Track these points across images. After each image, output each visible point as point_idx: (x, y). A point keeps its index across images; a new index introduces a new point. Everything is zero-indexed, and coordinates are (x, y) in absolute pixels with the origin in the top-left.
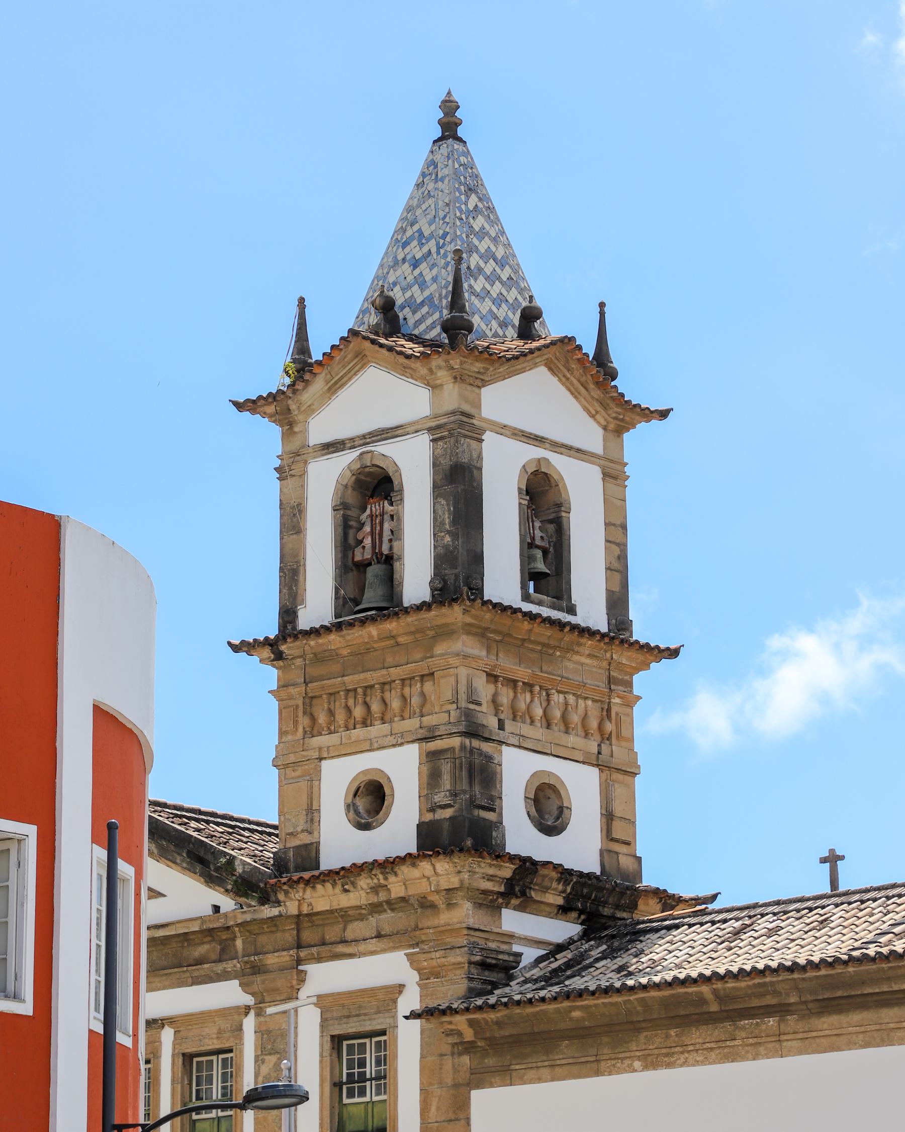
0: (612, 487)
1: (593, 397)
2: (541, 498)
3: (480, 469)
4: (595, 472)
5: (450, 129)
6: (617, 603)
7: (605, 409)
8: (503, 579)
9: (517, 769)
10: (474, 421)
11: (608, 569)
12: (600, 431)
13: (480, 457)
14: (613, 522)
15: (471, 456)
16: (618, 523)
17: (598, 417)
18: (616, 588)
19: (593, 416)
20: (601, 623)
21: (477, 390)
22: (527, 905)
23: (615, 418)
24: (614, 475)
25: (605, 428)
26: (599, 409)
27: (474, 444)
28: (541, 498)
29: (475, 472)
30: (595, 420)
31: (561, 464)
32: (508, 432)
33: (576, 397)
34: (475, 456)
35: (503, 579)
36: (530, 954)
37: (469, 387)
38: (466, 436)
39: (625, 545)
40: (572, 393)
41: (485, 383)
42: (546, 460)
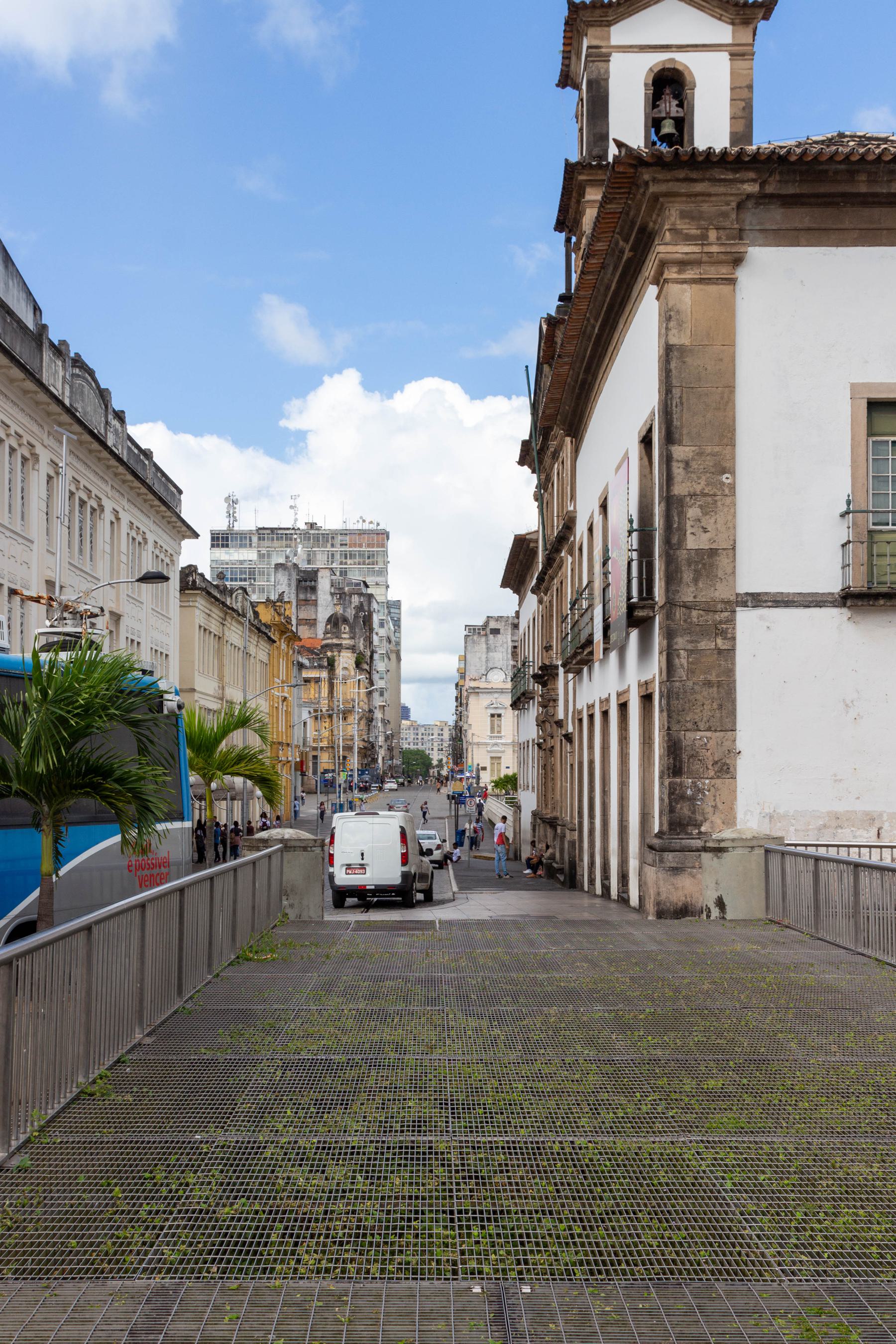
0: (741, 64)
1: (714, 6)
3: (607, 80)
4: (725, 56)
7: (726, 11)
10: (603, 50)
11: (733, 118)
12: (730, 27)
13: (607, 72)
14: (738, 85)
15: (599, 72)
16: (744, 84)
17: (723, 18)
18: (740, 128)
19: (720, 19)
21: (606, 29)
23: (738, 14)
25: (733, 24)
26: (721, 12)
27: (601, 65)
28: (669, 85)
29: (602, 82)
30: (723, 21)
31: (683, 59)
32: (636, 50)
33: (702, 10)
34: (602, 71)
37: (599, 29)
38: (593, 61)
39: (751, 99)
40: (698, 9)
41: (609, 24)
42: (672, 60)
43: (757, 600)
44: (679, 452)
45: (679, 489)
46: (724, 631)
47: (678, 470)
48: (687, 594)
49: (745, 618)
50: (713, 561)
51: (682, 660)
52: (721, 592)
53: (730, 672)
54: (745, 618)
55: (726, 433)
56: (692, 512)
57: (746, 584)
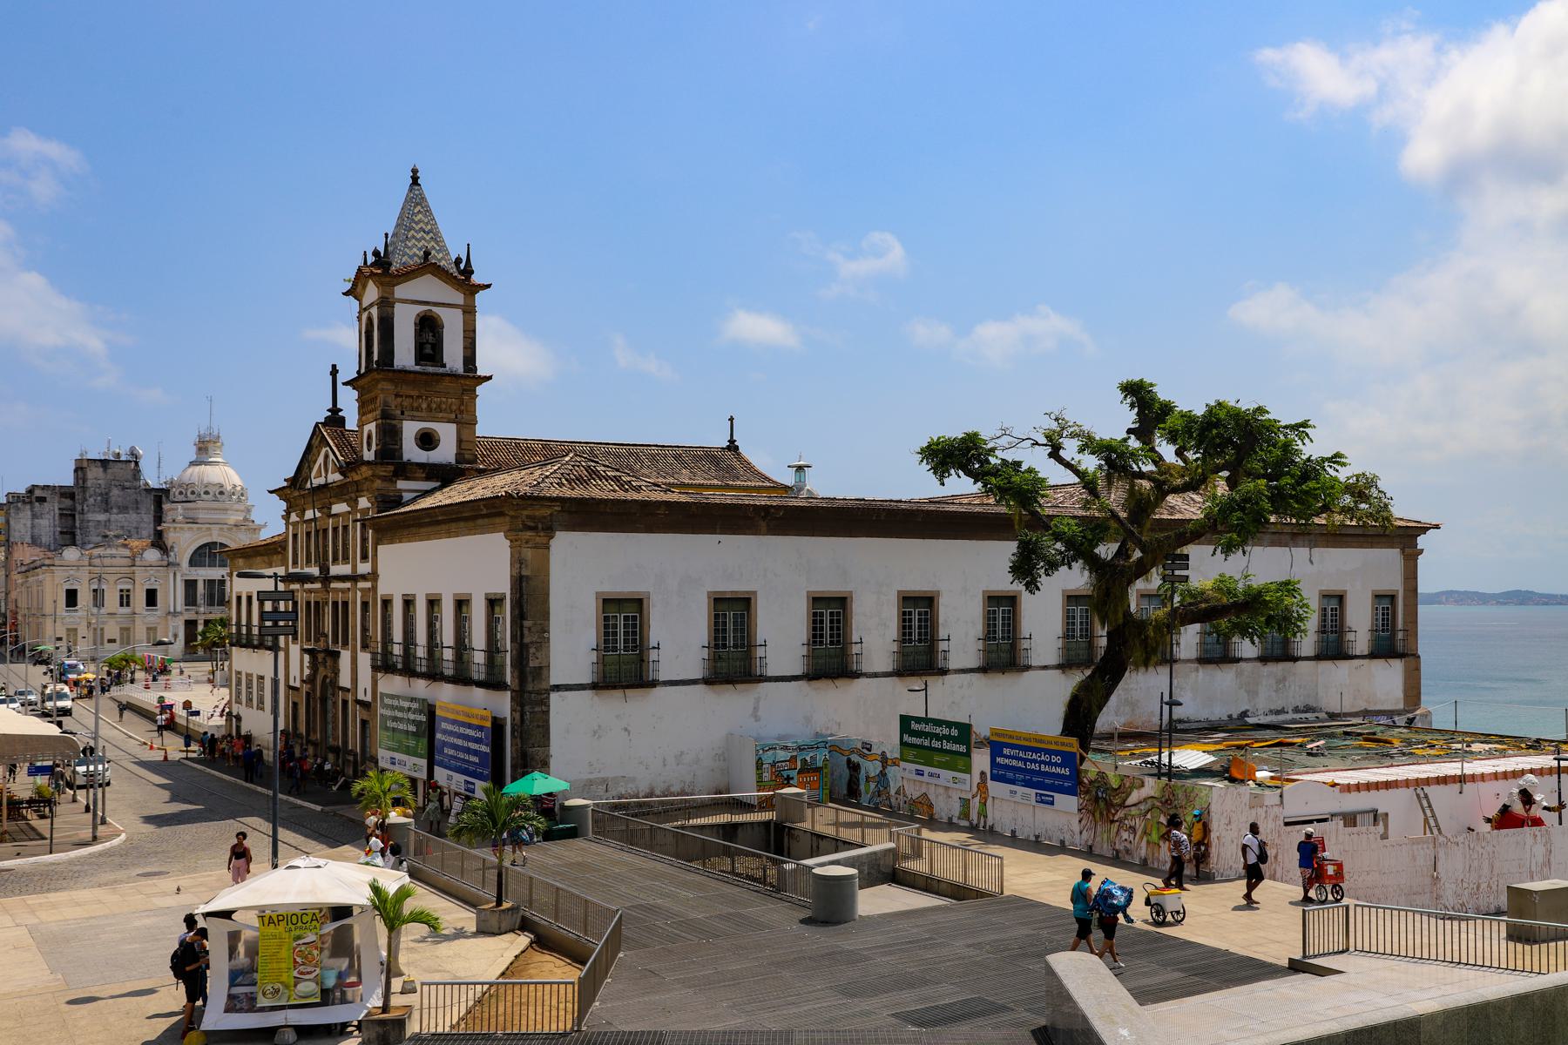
2: (428, 327)
4: (459, 312)
5: (415, 180)
6: (470, 360)
8: (404, 355)
9: (410, 429)
20: (461, 370)
22: (407, 479)
24: (469, 311)
28: (428, 327)
31: (435, 309)
35: (404, 355)
36: (407, 496)
43: (557, 688)
44: (527, 623)
45: (526, 640)
46: (545, 703)
47: (526, 632)
48: (530, 687)
49: (554, 696)
50: (542, 671)
51: (528, 716)
52: (544, 686)
53: (547, 721)
54: (554, 697)
55: (546, 615)
56: (532, 650)
57: (555, 679)
